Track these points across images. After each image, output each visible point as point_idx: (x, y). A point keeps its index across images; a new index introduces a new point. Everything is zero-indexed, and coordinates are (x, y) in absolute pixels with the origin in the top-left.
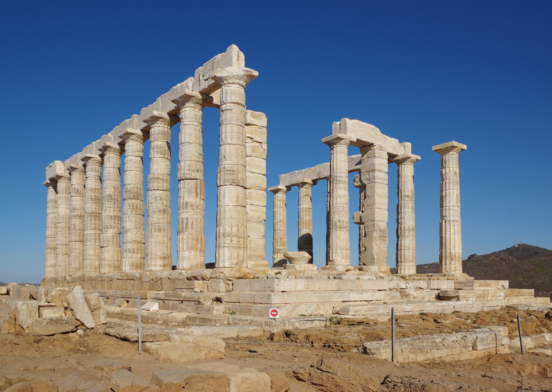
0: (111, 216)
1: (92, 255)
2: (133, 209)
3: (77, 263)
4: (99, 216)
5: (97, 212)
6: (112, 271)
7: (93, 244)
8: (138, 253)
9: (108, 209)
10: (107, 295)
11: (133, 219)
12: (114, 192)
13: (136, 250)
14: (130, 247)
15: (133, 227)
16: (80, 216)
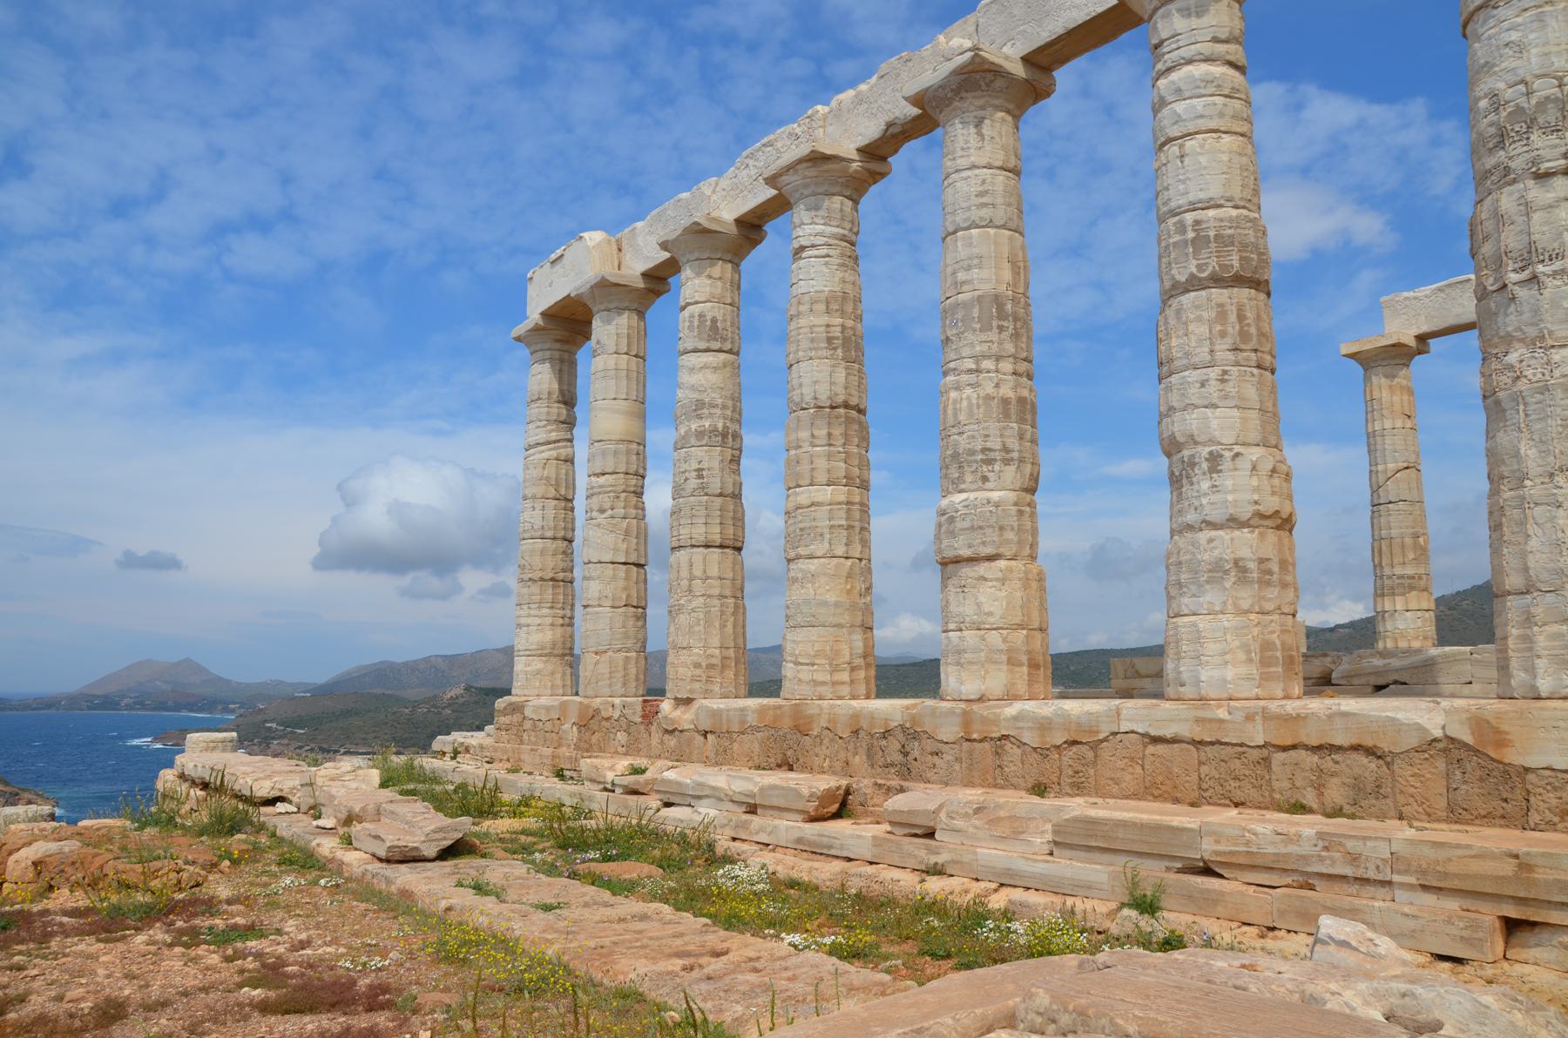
0: (1005, 402)
1: (836, 605)
2: (1244, 335)
3: (715, 641)
4: (860, 423)
5: (854, 401)
6: (1022, 688)
7: (840, 550)
8: (1284, 585)
9: (988, 364)
10: (1207, 849)
11: (1251, 393)
12: (1015, 285)
13: (1276, 569)
14: (1245, 552)
15: (1254, 436)
16: (724, 436)
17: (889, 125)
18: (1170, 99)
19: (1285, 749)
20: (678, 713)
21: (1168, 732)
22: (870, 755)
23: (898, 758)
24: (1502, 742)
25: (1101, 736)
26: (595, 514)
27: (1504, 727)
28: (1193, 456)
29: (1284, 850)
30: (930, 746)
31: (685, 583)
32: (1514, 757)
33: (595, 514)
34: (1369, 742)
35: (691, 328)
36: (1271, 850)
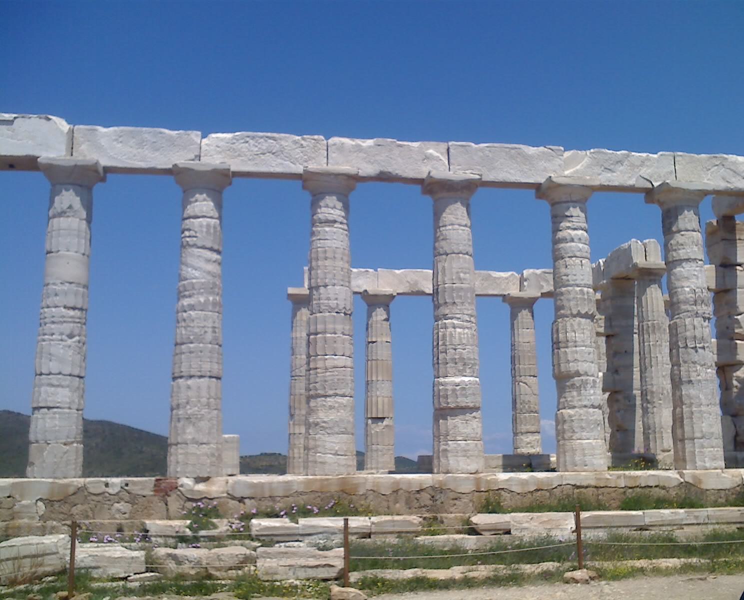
17: (382, 173)
18: (575, 240)
19: (630, 488)
20: (201, 487)
21: (585, 484)
22: (408, 502)
23: (429, 503)
24: (700, 481)
25: (554, 487)
26: (64, 337)
27: (701, 478)
28: (587, 380)
29: (674, 518)
30: (452, 495)
31: (204, 400)
32: (704, 487)
33: (64, 337)
34: (661, 484)
35: (208, 232)
36: (670, 518)
